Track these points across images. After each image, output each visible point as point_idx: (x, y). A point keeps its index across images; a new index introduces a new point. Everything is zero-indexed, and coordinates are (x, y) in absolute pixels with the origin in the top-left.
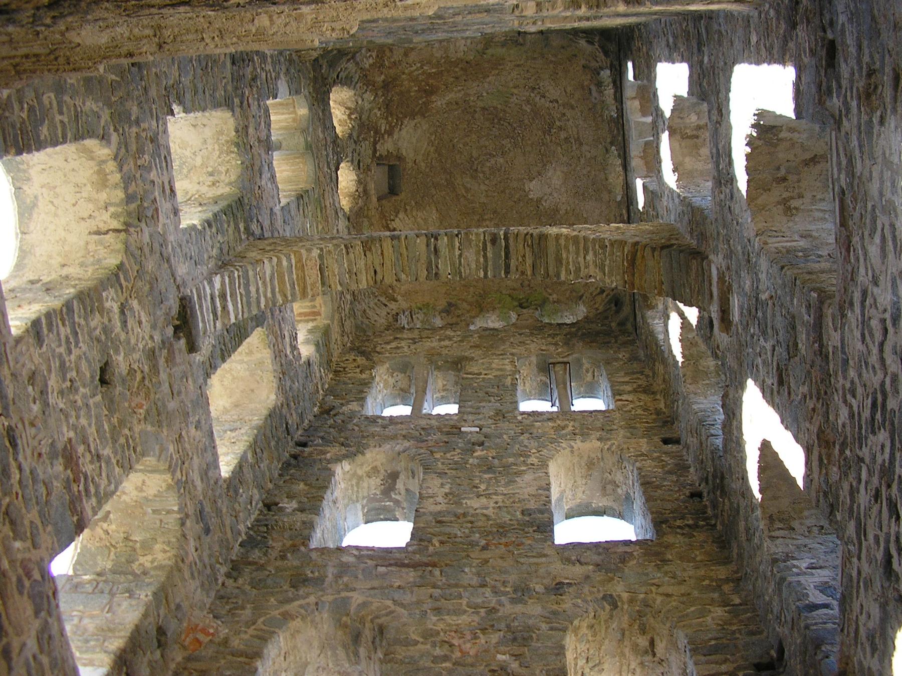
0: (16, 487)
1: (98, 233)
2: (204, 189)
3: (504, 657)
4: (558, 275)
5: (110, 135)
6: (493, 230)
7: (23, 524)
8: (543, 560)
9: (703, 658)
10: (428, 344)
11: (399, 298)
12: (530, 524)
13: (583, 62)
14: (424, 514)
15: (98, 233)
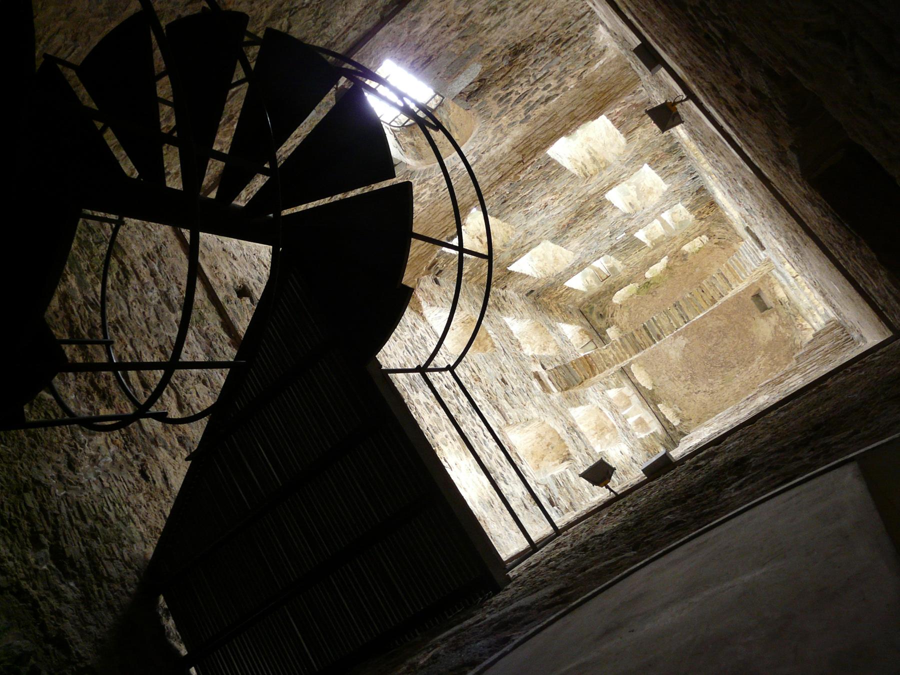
11: (715, 246)
13: (692, 422)
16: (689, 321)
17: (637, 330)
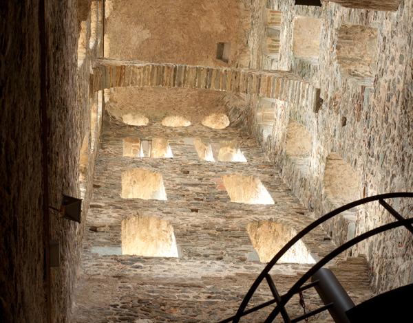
13: (117, 105)
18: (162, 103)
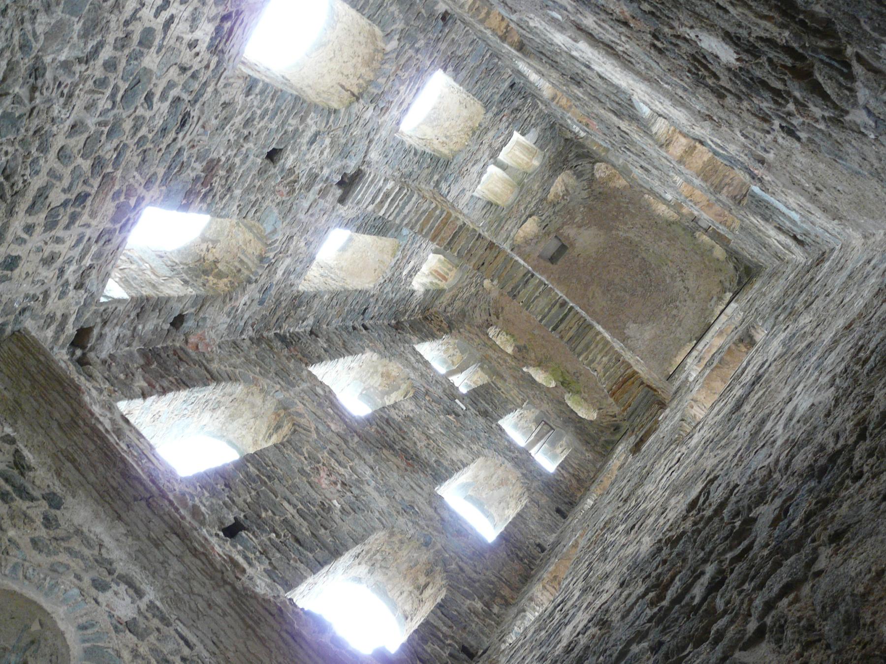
0: (164, 146)
1: (343, 87)
2: (436, 142)
3: (337, 504)
4: (579, 355)
5: (392, 38)
6: (567, 300)
7: (149, 168)
8: (418, 490)
9: (440, 614)
10: (490, 352)
11: (501, 318)
12: (433, 469)
13: (722, 278)
14: (385, 412)
15: (343, 87)
16: (529, 272)
17: (562, 337)
18: (668, 239)
